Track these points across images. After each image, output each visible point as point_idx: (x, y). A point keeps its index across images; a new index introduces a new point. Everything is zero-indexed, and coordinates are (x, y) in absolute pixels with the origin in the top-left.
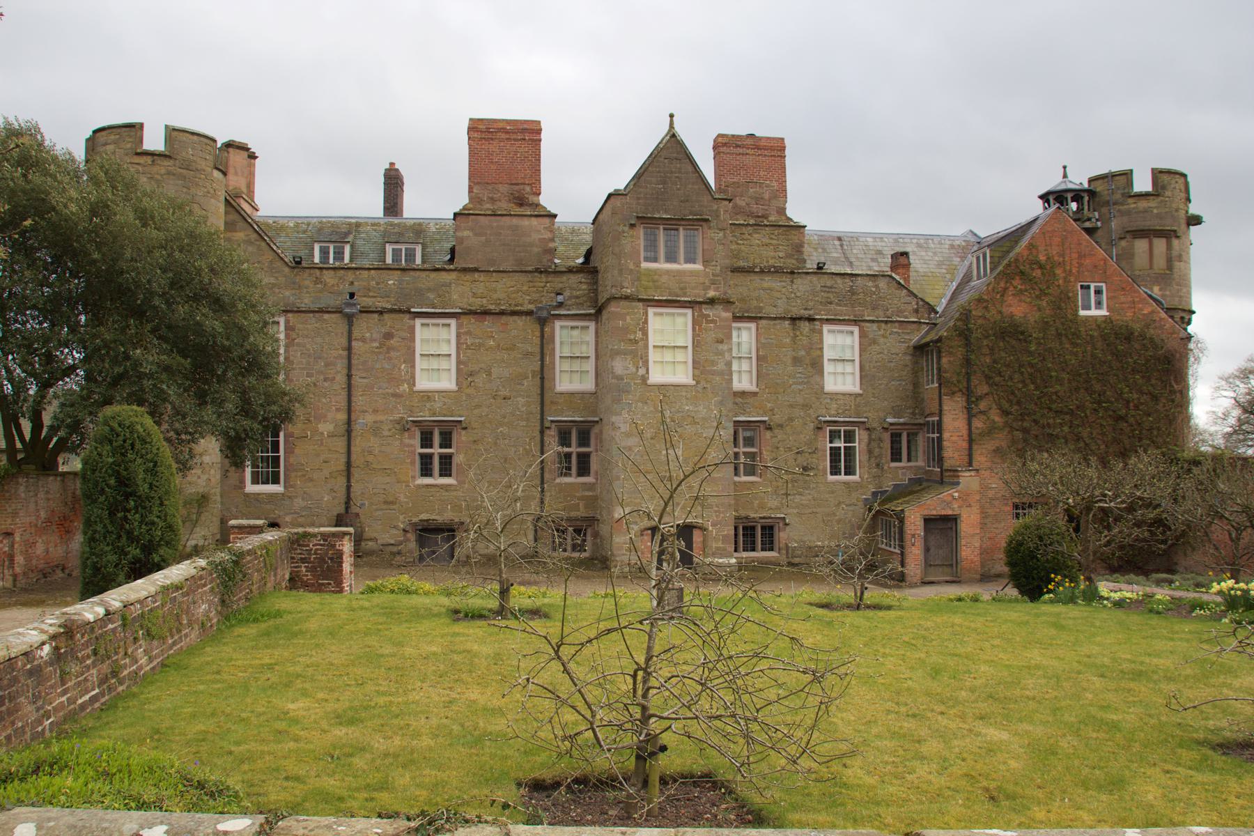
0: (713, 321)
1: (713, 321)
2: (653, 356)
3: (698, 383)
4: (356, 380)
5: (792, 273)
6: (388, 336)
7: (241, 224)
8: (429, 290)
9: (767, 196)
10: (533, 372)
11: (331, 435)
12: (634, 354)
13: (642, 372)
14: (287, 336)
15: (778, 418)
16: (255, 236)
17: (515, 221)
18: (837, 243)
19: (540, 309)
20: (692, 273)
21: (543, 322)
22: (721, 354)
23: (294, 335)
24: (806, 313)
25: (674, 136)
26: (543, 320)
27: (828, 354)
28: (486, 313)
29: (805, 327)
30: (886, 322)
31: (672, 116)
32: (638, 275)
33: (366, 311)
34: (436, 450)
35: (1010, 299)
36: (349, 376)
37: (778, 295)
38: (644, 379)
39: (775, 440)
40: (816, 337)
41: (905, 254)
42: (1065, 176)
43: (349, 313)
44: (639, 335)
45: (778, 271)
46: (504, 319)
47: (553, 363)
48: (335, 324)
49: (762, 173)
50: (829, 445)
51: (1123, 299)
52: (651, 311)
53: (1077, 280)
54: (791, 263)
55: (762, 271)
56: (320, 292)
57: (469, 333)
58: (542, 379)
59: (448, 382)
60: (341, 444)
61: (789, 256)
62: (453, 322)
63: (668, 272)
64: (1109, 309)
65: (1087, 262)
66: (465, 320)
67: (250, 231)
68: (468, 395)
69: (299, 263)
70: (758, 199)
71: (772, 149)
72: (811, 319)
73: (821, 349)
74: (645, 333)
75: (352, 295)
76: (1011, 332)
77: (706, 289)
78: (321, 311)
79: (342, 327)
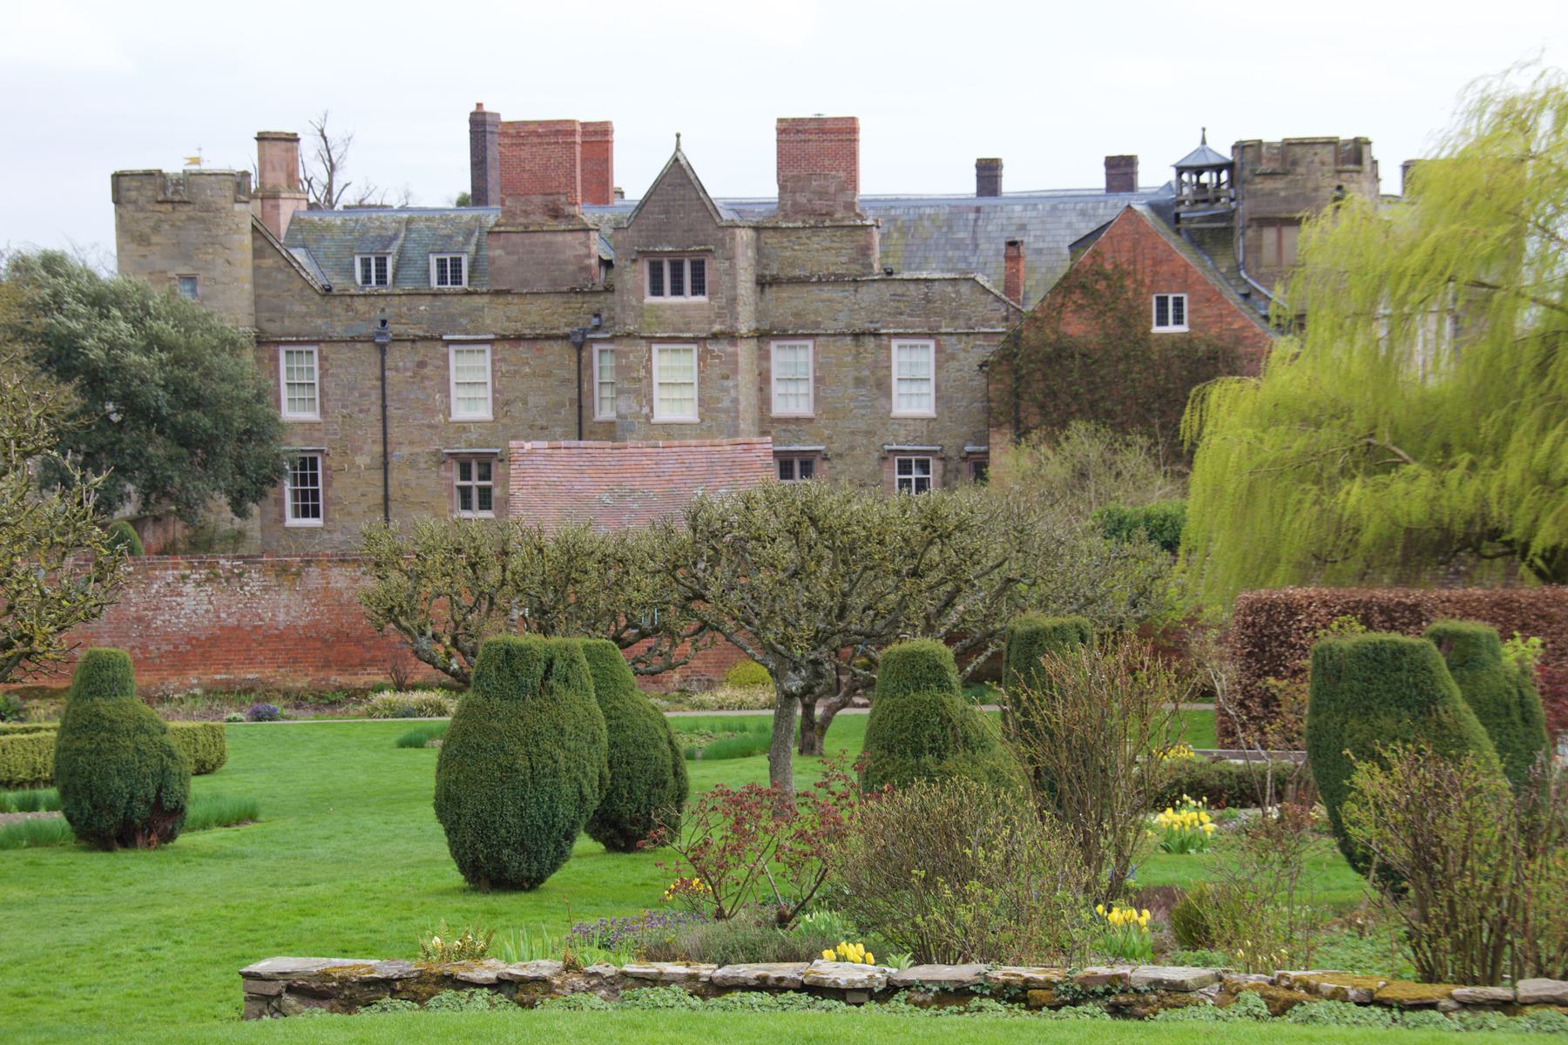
0: (718, 357)
1: (718, 357)
2: (658, 393)
3: (702, 420)
4: (391, 411)
5: (855, 281)
6: (422, 364)
7: (270, 250)
8: (461, 315)
9: (832, 190)
10: (571, 400)
11: (368, 468)
12: (637, 392)
13: (646, 410)
14: (321, 367)
15: (836, 447)
16: (283, 262)
17: (548, 237)
18: (972, 216)
19: (574, 333)
20: (699, 307)
21: (580, 347)
22: (727, 390)
23: (327, 365)
24: (872, 326)
25: (677, 160)
26: (580, 343)
27: (895, 374)
28: (519, 338)
29: (870, 343)
30: (968, 334)
31: (678, 136)
32: (641, 312)
33: (398, 340)
34: (475, 483)
35: (1068, 316)
36: (384, 407)
37: (840, 307)
38: (648, 418)
39: (833, 471)
40: (882, 355)
41: (1012, 244)
42: (1204, 142)
43: (381, 342)
44: (643, 373)
45: (838, 280)
46: (540, 344)
47: (592, 390)
48: (367, 353)
49: (827, 162)
50: (898, 477)
51: (1207, 312)
52: (655, 348)
53: (1151, 292)
54: (855, 269)
55: (820, 281)
56: (352, 319)
57: (503, 360)
58: (580, 407)
59: (484, 412)
60: (377, 477)
61: (853, 261)
62: (488, 348)
63: (671, 307)
64: (1191, 325)
65: (1164, 268)
66: (499, 347)
67: (279, 258)
68: (505, 426)
69: (330, 290)
70: (822, 194)
71: (839, 131)
72: (876, 335)
73: (889, 368)
74: (649, 371)
75: (384, 323)
76: (1059, 355)
77: (711, 323)
78: (353, 340)
79: (376, 357)
